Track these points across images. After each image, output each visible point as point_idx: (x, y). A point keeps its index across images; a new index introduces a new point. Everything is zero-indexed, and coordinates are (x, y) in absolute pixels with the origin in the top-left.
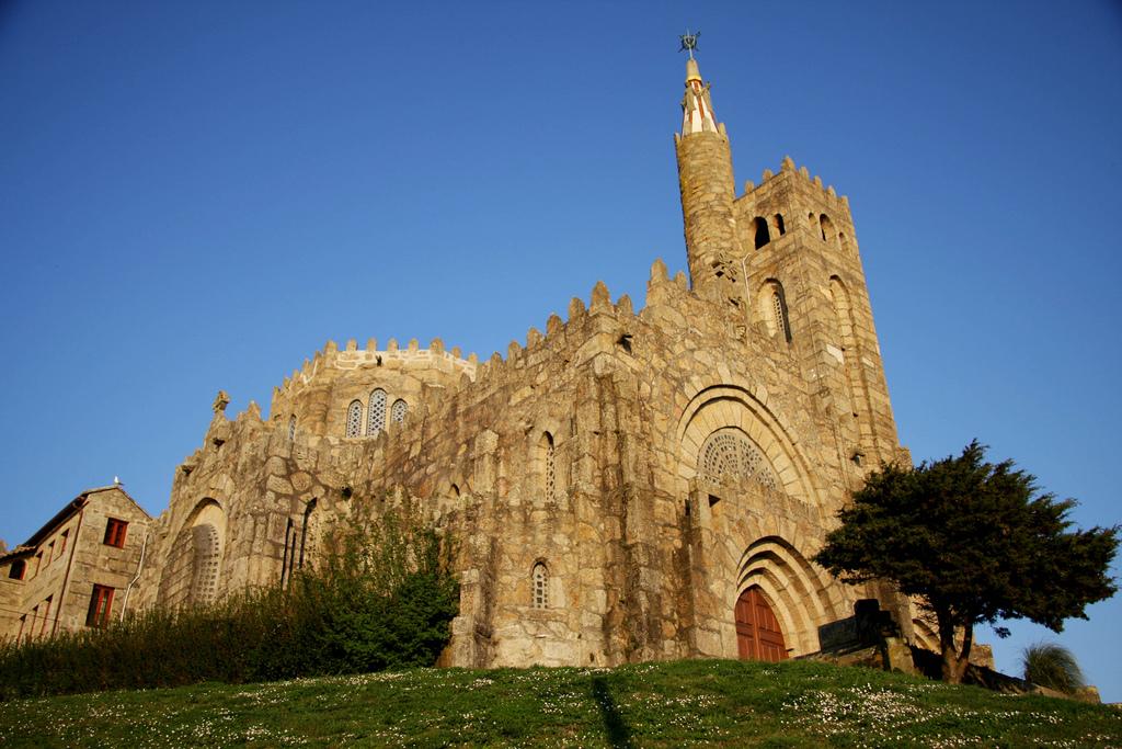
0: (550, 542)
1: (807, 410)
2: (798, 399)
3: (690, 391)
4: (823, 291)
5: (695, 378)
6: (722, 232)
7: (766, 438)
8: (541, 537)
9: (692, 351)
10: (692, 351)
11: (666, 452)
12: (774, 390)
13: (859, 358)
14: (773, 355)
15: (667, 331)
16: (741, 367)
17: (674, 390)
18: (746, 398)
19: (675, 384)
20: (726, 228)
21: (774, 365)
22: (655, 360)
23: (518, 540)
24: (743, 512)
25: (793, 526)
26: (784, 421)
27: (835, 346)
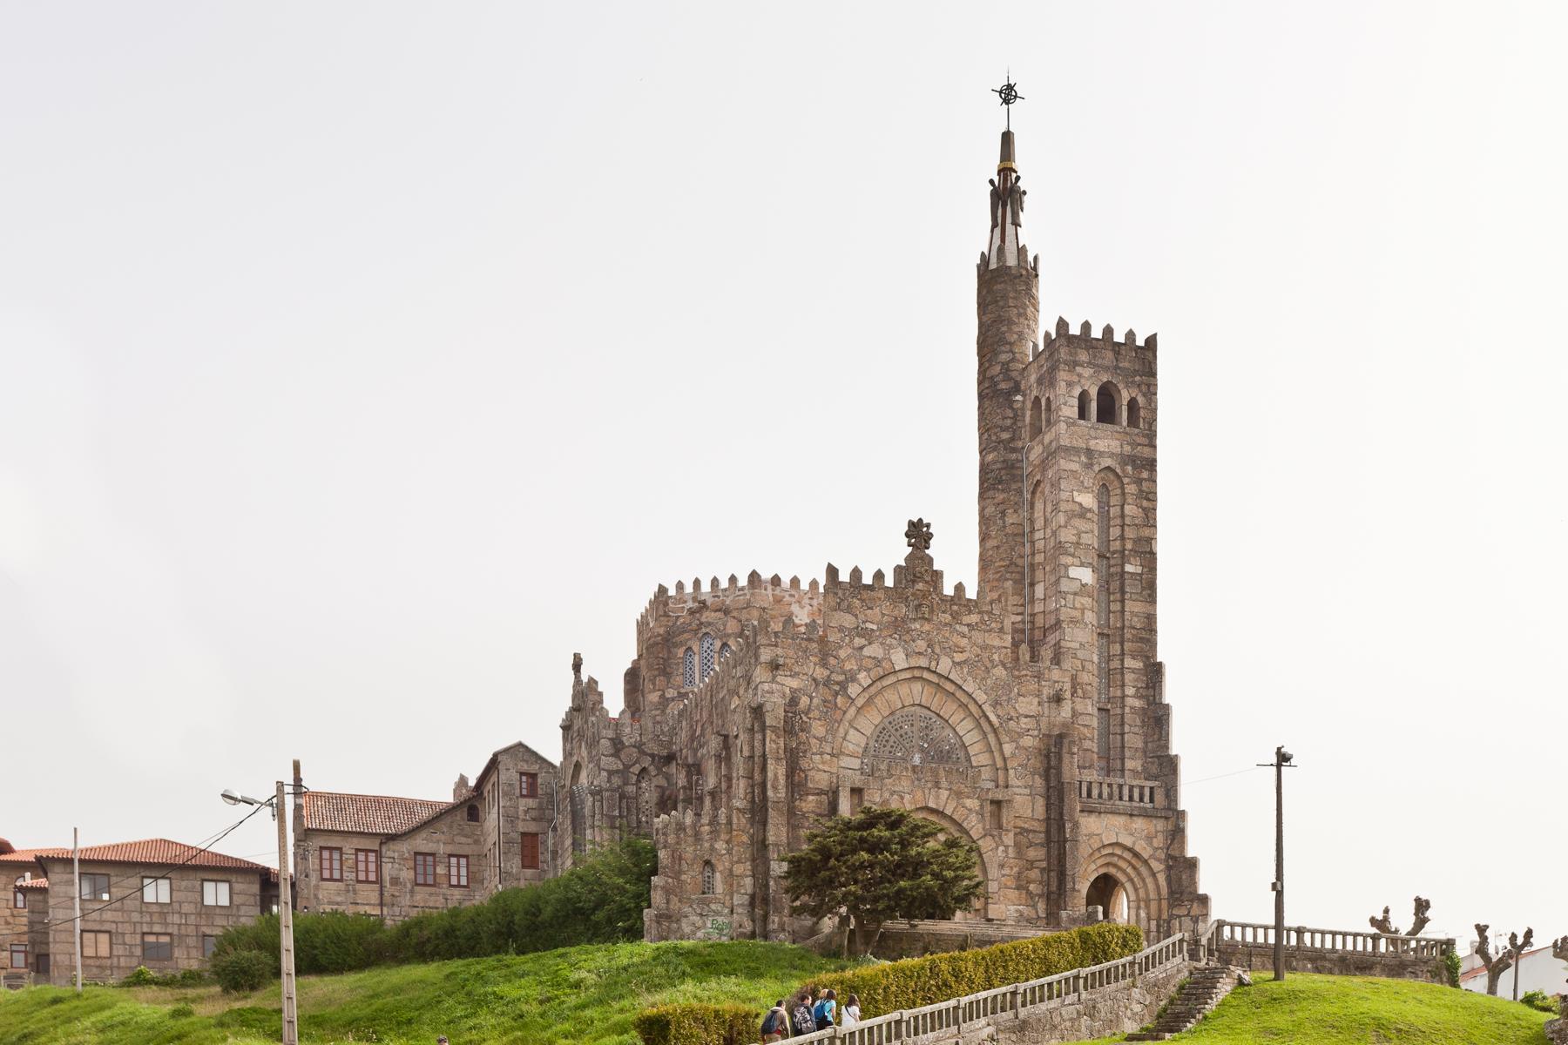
0: (712, 849)
1: (1004, 665)
2: (996, 657)
3: (853, 690)
4: (1078, 499)
5: (862, 676)
6: (1004, 418)
7: (949, 709)
8: (707, 845)
9: (861, 648)
10: (861, 648)
11: (822, 754)
12: (958, 657)
13: (1123, 566)
14: (966, 620)
15: (833, 637)
16: (921, 645)
17: (837, 693)
18: (926, 675)
19: (837, 688)
20: (1010, 413)
21: (965, 629)
22: (820, 673)
23: (690, 849)
24: (887, 795)
25: (944, 794)
26: (970, 687)
27: (1082, 565)
